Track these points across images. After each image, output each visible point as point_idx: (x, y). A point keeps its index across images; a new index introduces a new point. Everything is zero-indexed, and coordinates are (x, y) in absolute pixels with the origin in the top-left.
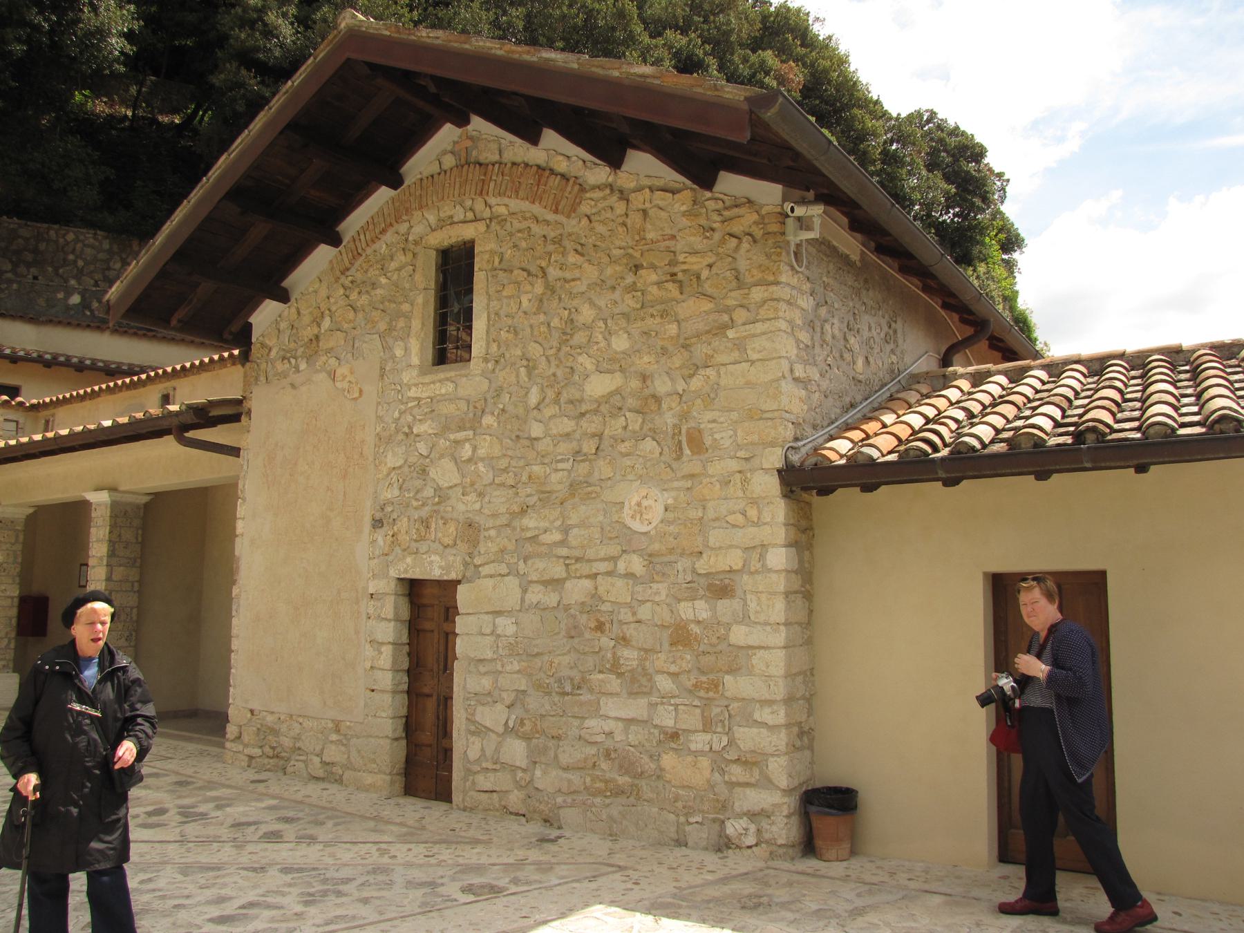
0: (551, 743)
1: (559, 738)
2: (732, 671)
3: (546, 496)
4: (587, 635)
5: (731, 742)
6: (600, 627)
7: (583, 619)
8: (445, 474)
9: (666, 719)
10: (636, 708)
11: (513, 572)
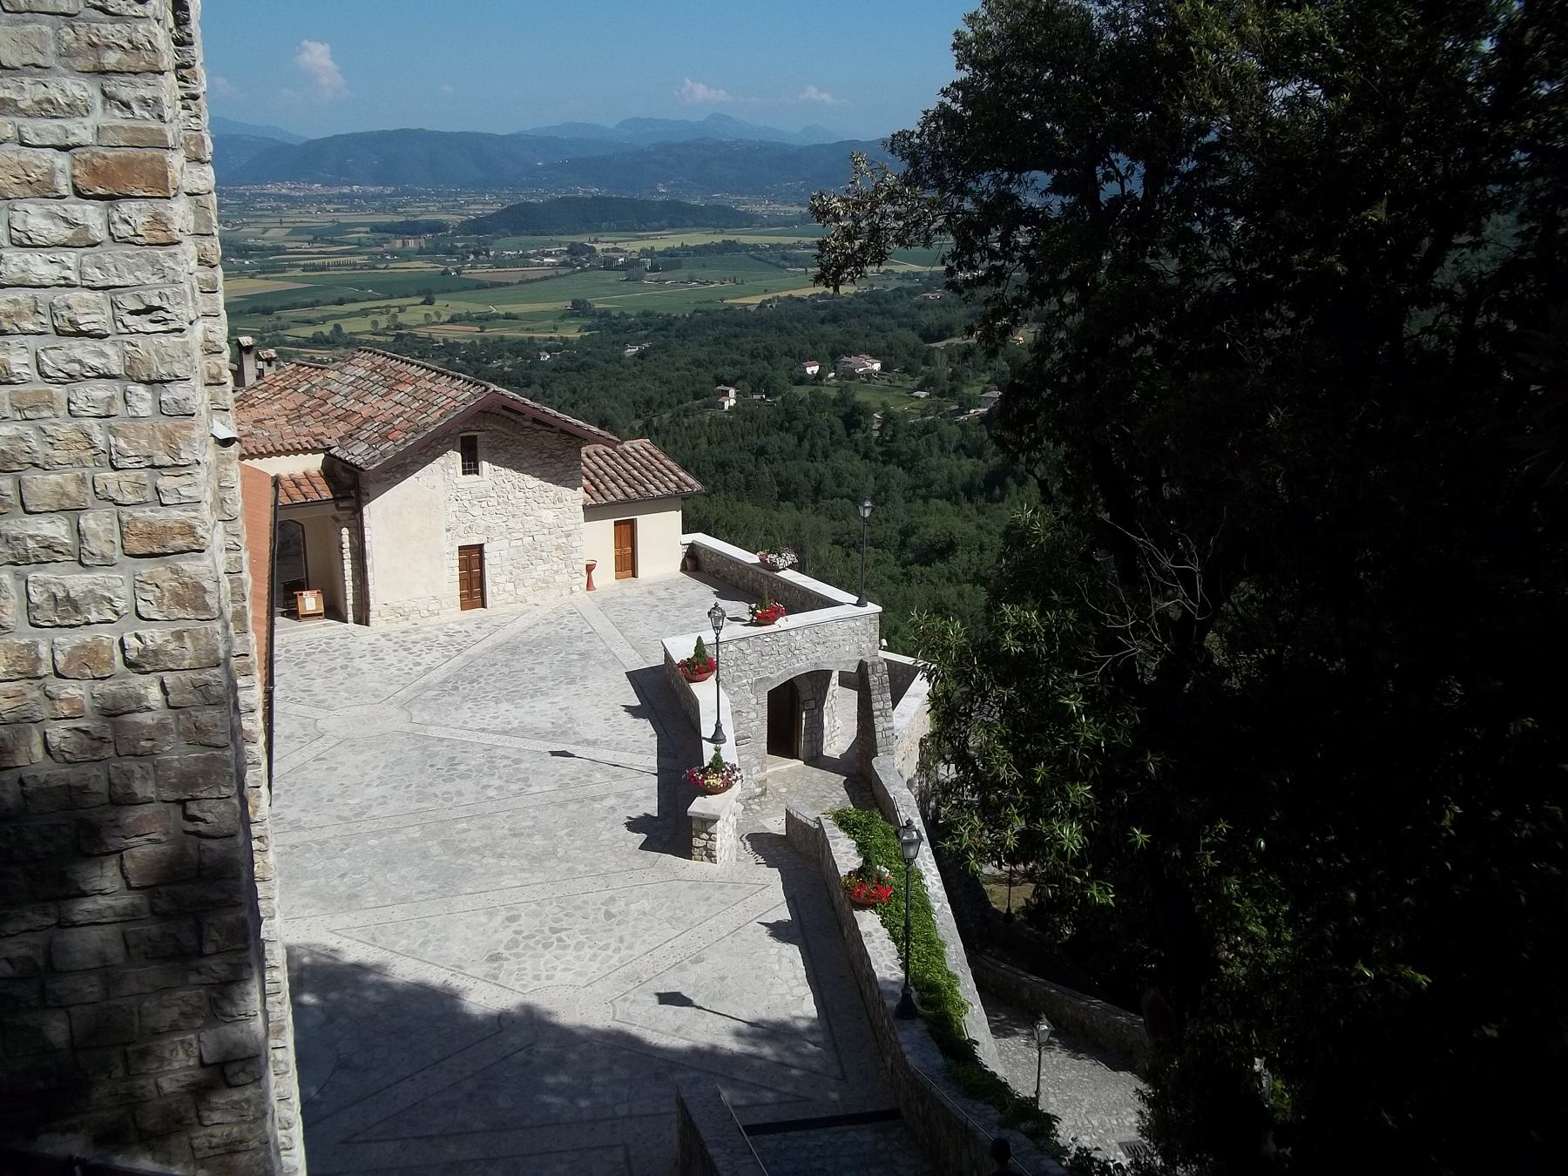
6: (536, 549)
8: (477, 511)
9: (555, 568)
10: (547, 566)
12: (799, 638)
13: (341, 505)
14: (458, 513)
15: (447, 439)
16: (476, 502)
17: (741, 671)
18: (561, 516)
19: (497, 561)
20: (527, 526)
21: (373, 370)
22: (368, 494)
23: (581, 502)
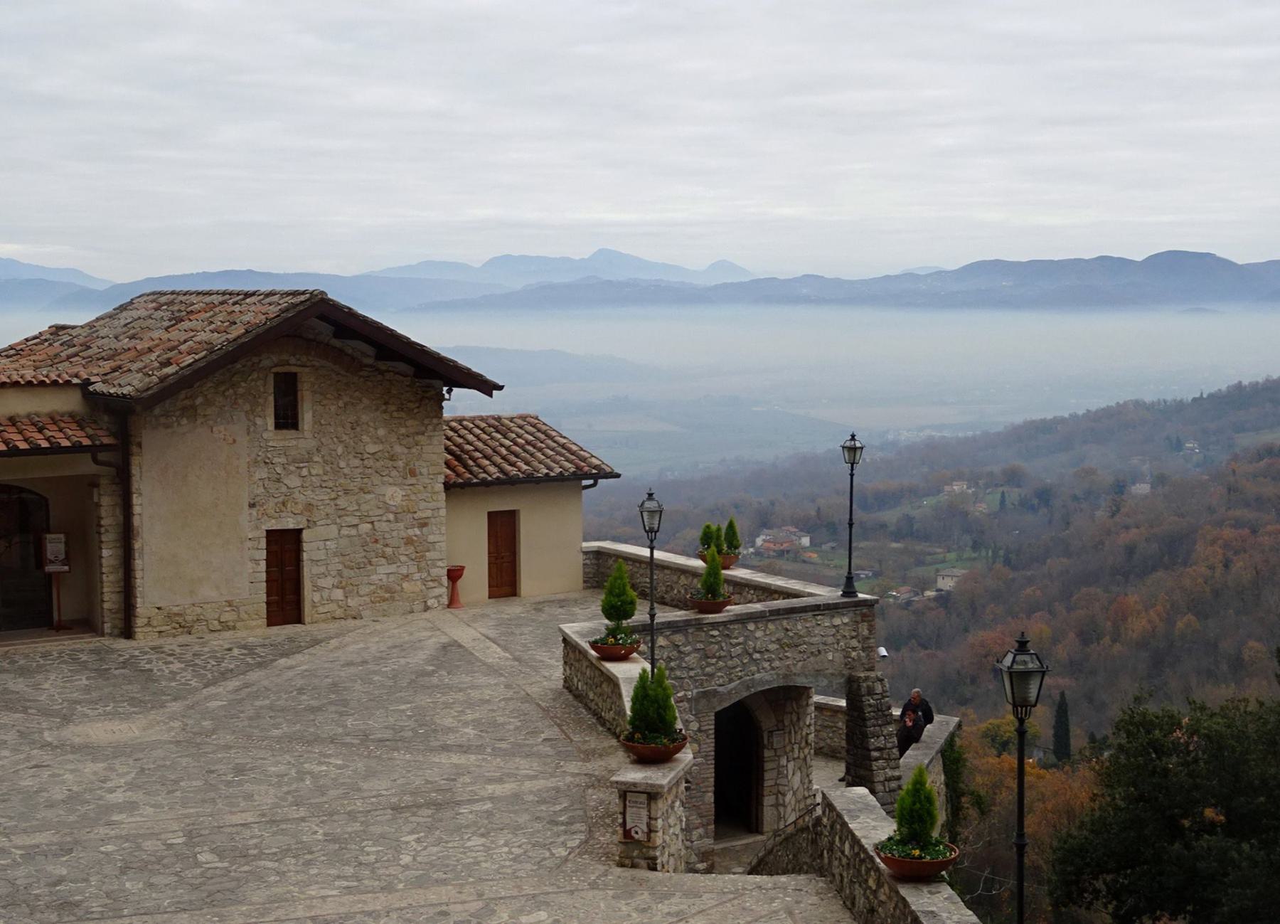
0: (355, 588)
1: (358, 585)
2: (428, 551)
3: (346, 492)
4: (370, 545)
5: (429, 574)
6: (376, 541)
7: (368, 539)
8: (293, 481)
10: (393, 568)
11: (336, 524)
12: (759, 634)
13: (102, 456)
14: (266, 482)
15: (255, 375)
16: (292, 468)
17: (677, 678)
18: (413, 497)
19: (321, 555)
20: (364, 507)
21: (156, 309)
22: (140, 445)
23: (441, 479)
